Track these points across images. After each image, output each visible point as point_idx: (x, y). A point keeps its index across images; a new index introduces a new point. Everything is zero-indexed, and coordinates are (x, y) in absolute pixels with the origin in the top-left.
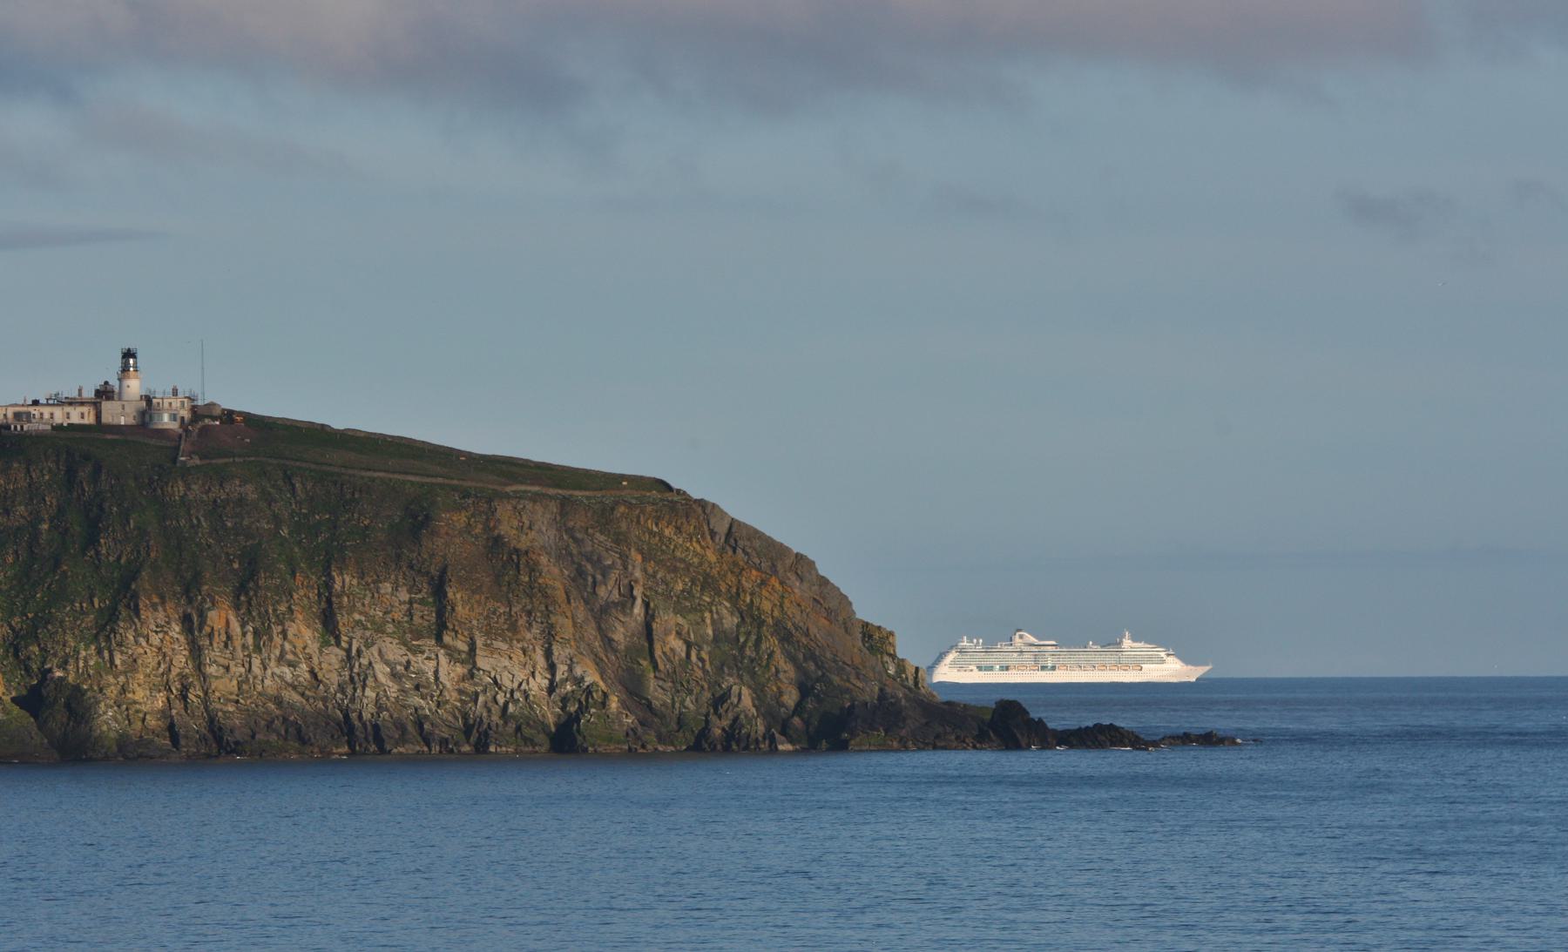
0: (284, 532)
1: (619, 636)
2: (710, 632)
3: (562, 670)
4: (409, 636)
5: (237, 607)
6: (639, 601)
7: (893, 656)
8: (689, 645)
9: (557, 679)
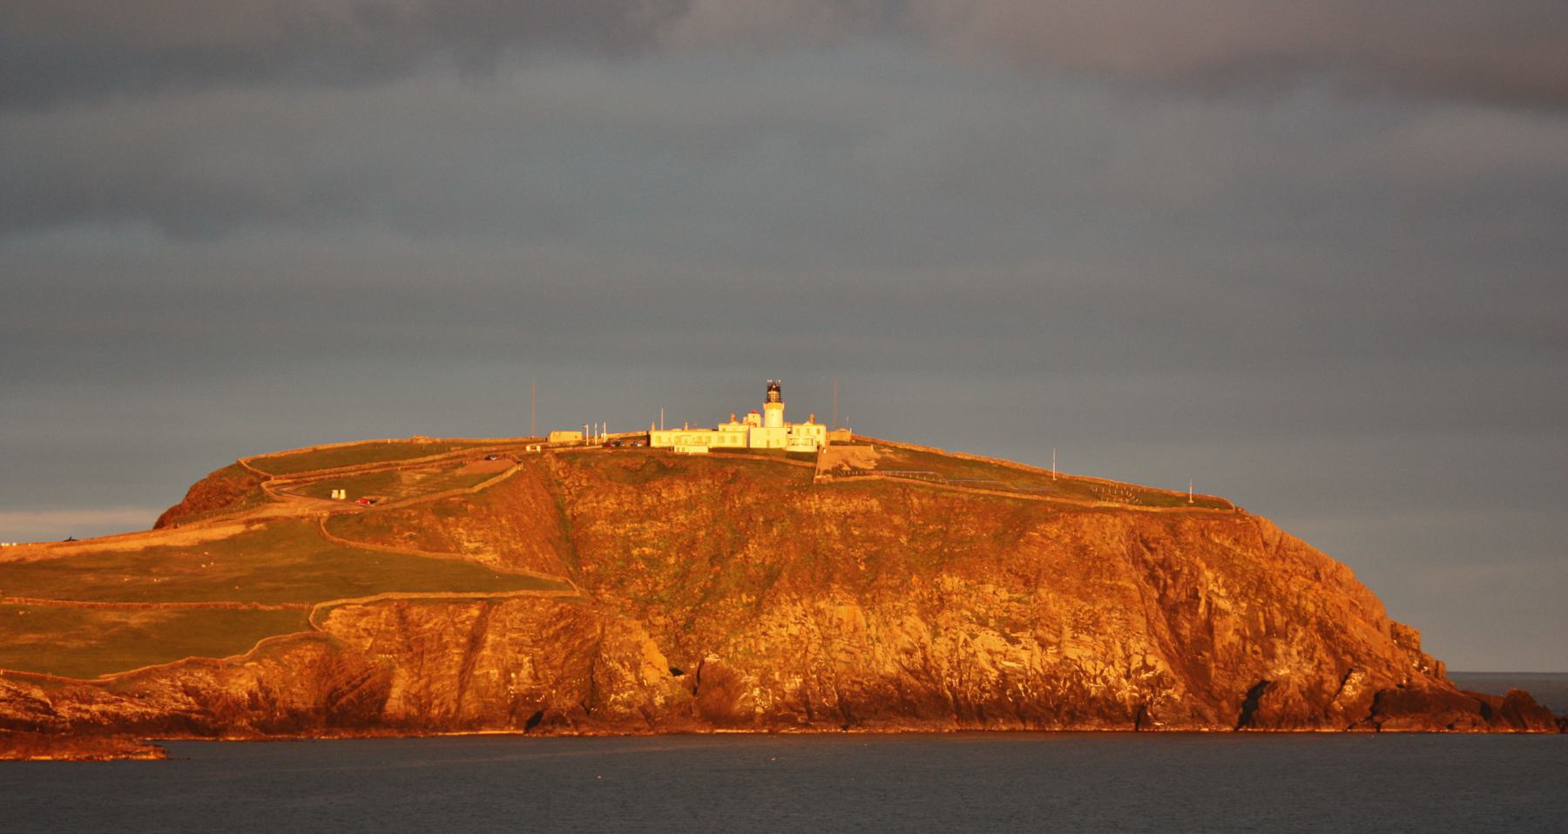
0: (903, 540)
1: (1186, 630)
2: (1263, 629)
3: (1136, 662)
4: (1010, 629)
5: (861, 602)
6: (1203, 602)
7: (1418, 651)
8: (1244, 638)
9: (1133, 667)
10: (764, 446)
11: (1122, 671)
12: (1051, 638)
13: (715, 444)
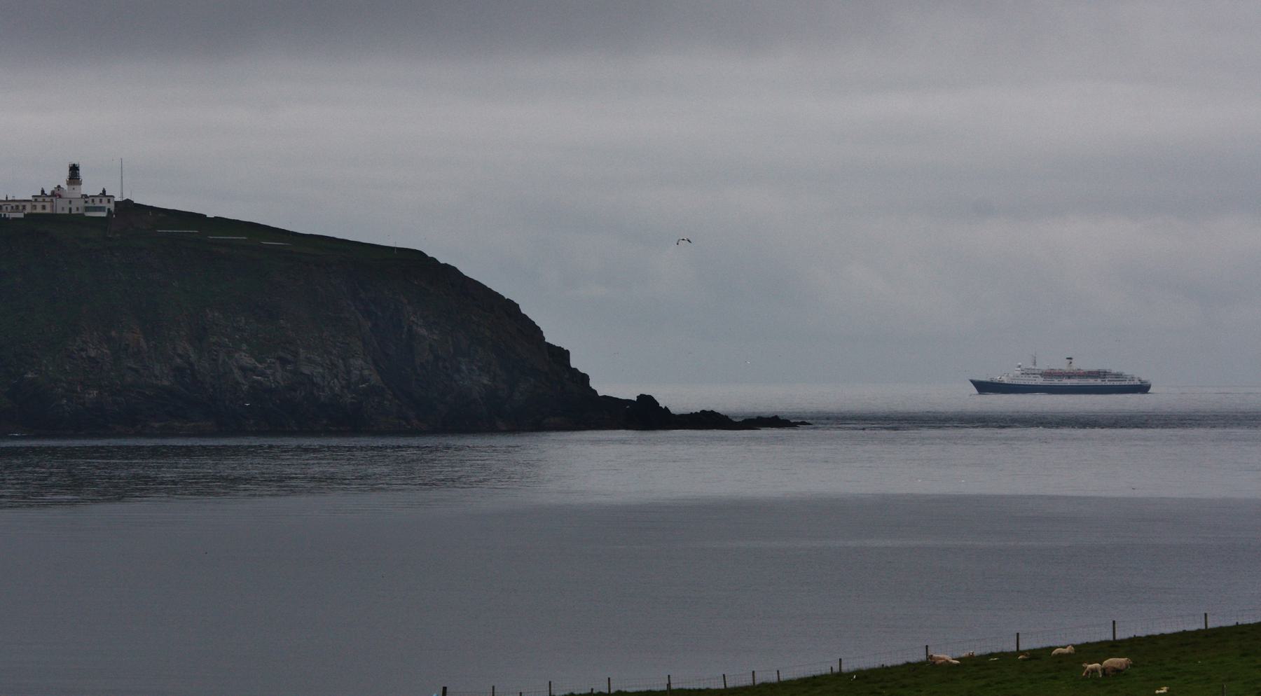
10: (67, 212)
12: (289, 357)
13: (28, 210)
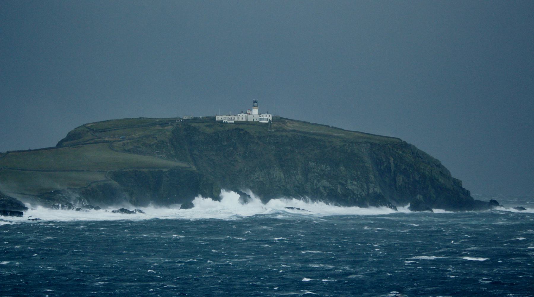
7: (461, 187)
11: (366, 193)
13: (236, 119)
